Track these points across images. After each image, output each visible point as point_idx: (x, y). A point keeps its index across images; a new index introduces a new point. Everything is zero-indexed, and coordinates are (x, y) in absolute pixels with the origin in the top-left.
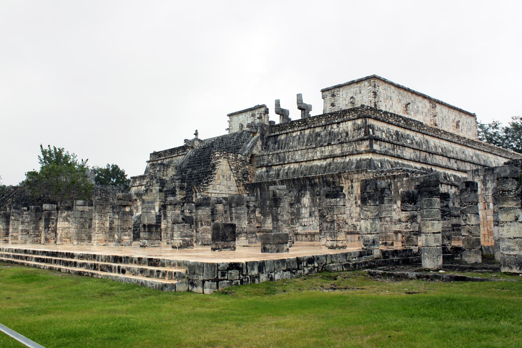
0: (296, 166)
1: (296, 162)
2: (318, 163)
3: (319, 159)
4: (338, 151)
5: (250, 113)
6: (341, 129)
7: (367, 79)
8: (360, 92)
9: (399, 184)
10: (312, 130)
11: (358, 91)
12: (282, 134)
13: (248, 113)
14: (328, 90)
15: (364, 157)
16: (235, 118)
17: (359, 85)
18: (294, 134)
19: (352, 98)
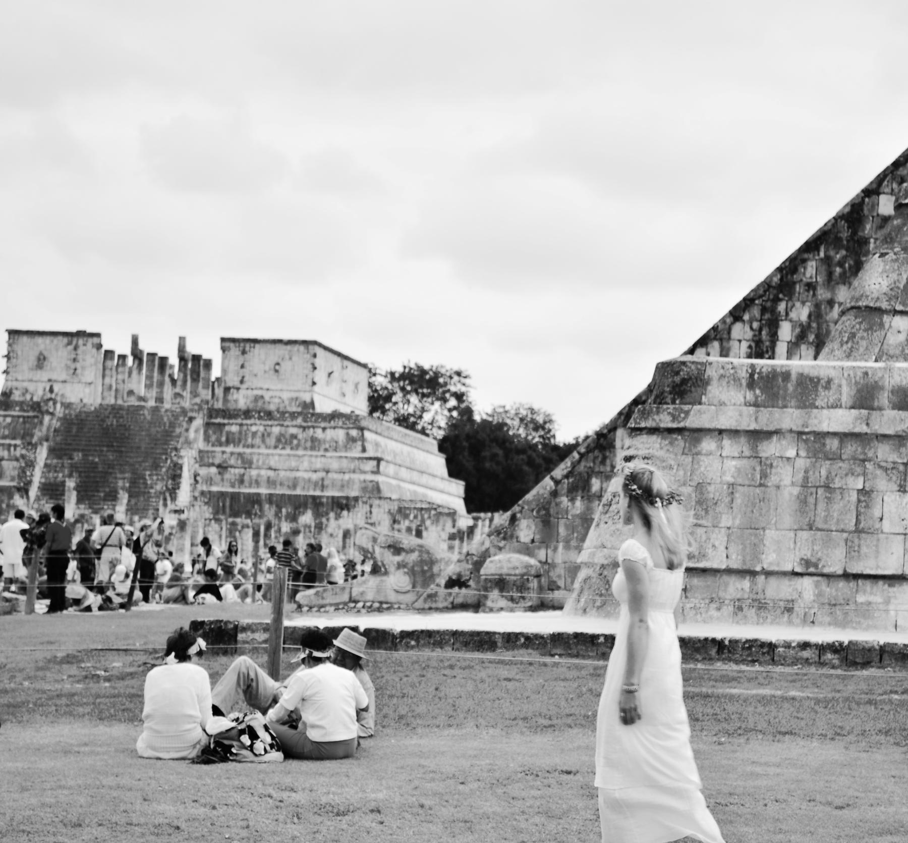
0: (271, 473)
1: (270, 469)
2: (306, 475)
3: (306, 471)
4: (335, 465)
5: (65, 340)
6: (328, 438)
7: (305, 343)
8: (290, 359)
9: (426, 516)
10: (283, 428)
11: (287, 357)
12: (232, 424)
13: (60, 338)
14: (233, 340)
15: (370, 477)
16: (25, 339)
17: (289, 347)
18: (254, 429)
19: (278, 364)
